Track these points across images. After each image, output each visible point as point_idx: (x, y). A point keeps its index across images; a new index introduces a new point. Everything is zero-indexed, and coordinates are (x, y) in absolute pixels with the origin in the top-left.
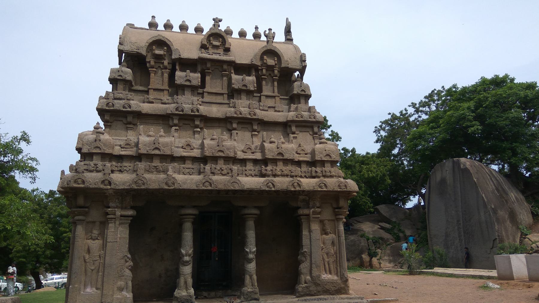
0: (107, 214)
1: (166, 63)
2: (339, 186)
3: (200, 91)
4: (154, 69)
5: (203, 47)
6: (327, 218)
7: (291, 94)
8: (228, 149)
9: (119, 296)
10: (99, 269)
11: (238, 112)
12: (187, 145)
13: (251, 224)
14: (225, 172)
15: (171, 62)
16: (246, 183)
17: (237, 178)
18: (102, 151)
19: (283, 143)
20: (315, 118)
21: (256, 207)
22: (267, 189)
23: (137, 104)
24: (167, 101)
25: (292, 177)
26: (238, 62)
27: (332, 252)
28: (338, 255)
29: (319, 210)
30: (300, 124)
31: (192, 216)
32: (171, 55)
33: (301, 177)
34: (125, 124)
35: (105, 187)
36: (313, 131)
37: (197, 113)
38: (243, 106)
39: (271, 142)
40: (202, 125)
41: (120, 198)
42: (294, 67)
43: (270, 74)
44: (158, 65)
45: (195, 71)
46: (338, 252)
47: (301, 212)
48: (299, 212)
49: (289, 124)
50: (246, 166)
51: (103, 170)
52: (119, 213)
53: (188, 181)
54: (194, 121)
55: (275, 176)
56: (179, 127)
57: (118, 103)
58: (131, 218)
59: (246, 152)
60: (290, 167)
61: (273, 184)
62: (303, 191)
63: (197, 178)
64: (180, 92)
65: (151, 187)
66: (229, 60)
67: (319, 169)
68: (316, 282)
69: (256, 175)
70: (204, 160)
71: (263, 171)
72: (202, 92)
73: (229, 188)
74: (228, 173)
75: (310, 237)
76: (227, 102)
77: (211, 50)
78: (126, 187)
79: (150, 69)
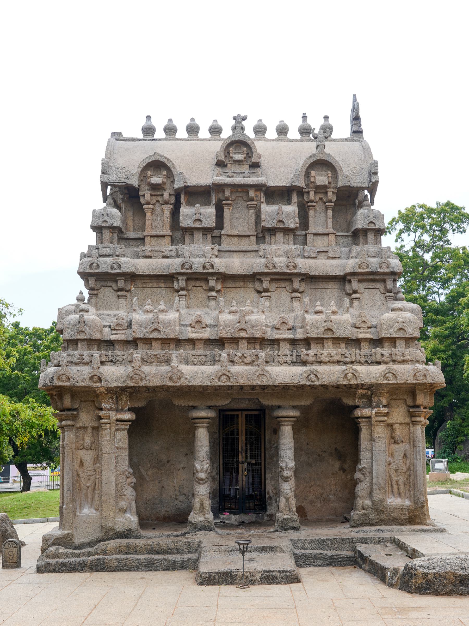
0: (100, 418)
1: (166, 196)
3: (217, 233)
4: (151, 206)
5: (220, 164)
7: (353, 229)
8: (253, 326)
9: (121, 520)
10: (95, 486)
11: (270, 265)
12: (197, 322)
13: (287, 431)
14: (248, 360)
15: (173, 193)
16: (277, 376)
17: (267, 368)
18: (87, 337)
19: (334, 313)
20: (388, 267)
21: (294, 407)
22: (308, 383)
23: (130, 263)
24: (170, 254)
25: (346, 363)
26: (271, 184)
27: (405, 469)
28: (412, 472)
29: (386, 410)
30: (365, 277)
32: (173, 182)
33: (360, 362)
34: (115, 290)
35: (95, 385)
36: (385, 287)
37: (211, 271)
38: (279, 254)
39: (316, 313)
40: (219, 287)
41: (115, 397)
42: (359, 185)
43: (321, 199)
45: (207, 203)
46: (412, 468)
47: (358, 413)
48: (355, 413)
49: (348, 278)
50: (279, 350)
51: (91, 362)
52: (114, 416)
53: (199, 375)
54: (207, 281)
55: (320, 363)
56: (188, 290)
57: (105, 263)
58: (130, 423)
59: (279, 329)
61: (316, 376)
62: (362, 385)
64: (187, 238)
65: (151, 384)
66: (256, 183)
67: (386, 350)
68: (378, 508)
69: (293, 363)
70: (220, 342)
71: (302, 356)
72: (218, 235)
73: (254, 384)
74: (253, 361)
75: (372, 449)
76: (255, 247)
78: (120, 385)
79: (144, 207)
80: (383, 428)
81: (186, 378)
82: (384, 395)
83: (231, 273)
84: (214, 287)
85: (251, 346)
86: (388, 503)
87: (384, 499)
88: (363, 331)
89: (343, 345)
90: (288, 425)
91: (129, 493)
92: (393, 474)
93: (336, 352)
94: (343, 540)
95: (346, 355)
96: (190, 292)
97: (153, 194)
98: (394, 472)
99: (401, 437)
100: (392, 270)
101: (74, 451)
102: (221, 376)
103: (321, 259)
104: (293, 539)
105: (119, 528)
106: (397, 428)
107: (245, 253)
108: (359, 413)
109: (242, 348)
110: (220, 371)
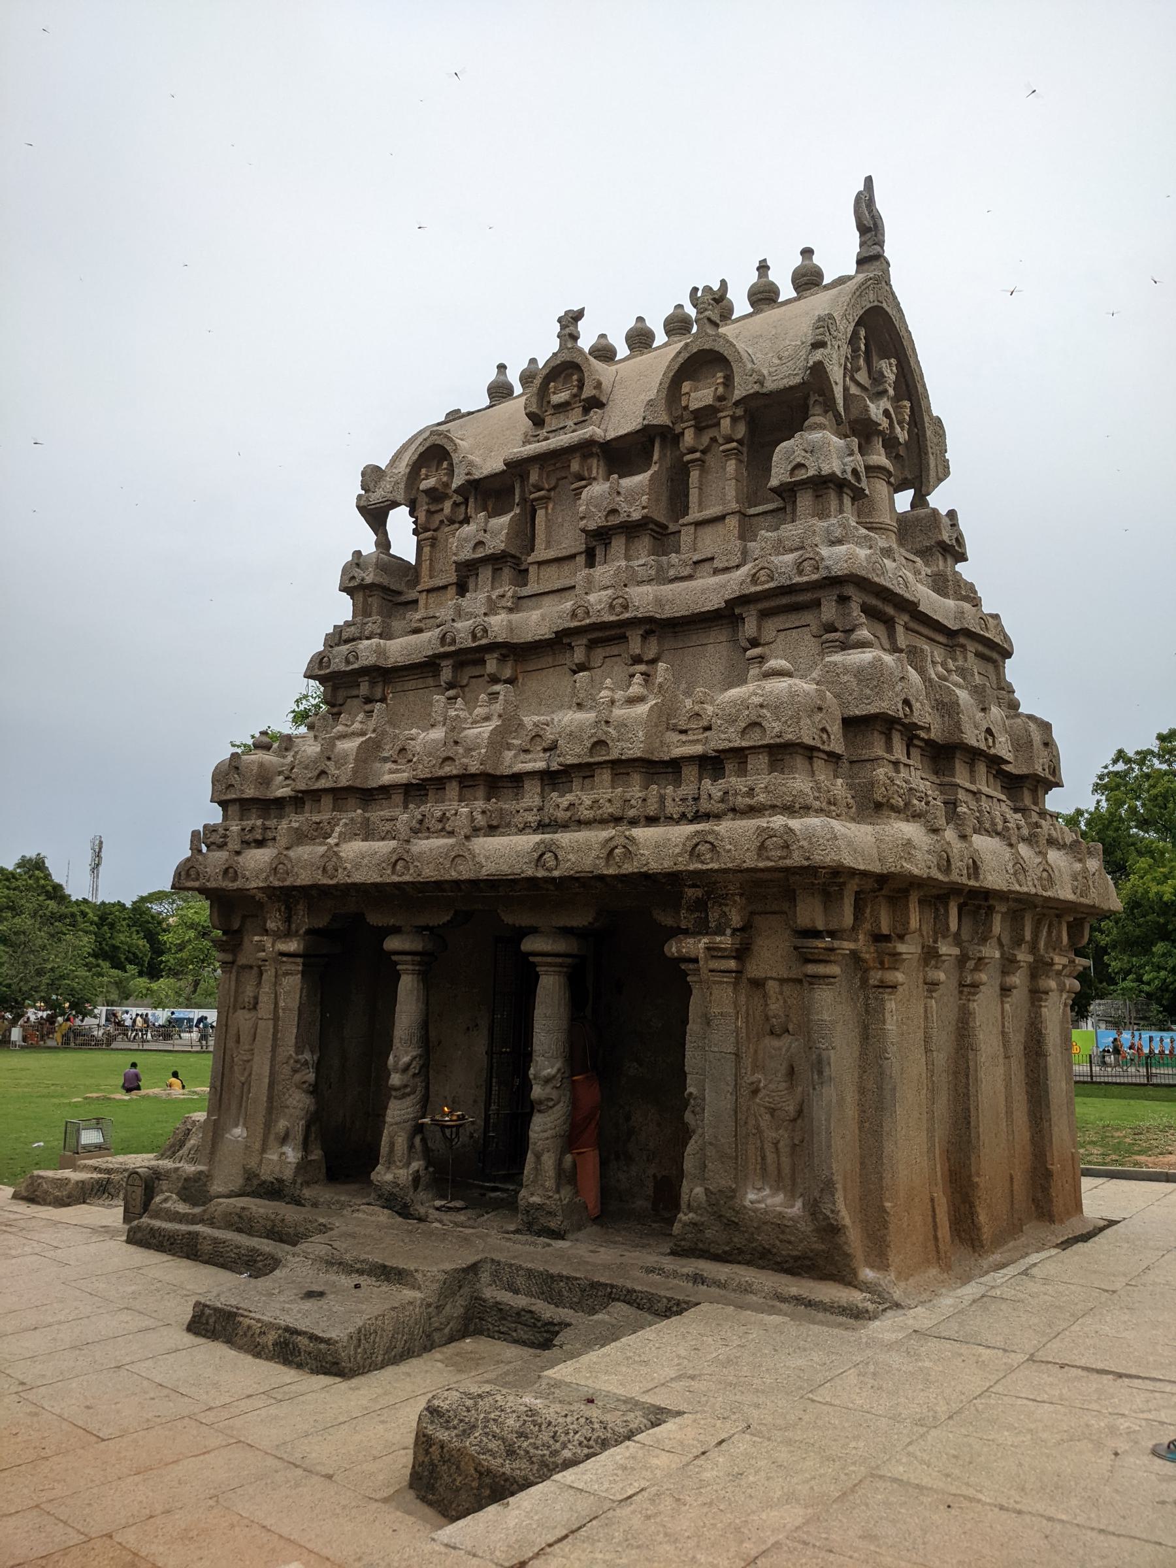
2: (762, 847)
4: (428, 534)
6: (774, 975)
8: (469, 750)
16: (487, 858)
22: (541, 873)
27: (791, 1108)
31: (409, 958)
37: (484, 641)
40: (507, 673)
44: (438, 518)
48: (666, 949)
49: (737, 611)
63: (384, 847)
65: (298, 883)
68: (724, 1209)
73: (447, 877)
77: (552, 422)
78: (261, 885)
80: (730, 990)
81: (345, 869)
82: (735, 902)
83: (522, 641)
84: (494, 675)
85: (467, 793)
86: (747, 1203)
88: (691, 738)
89: (636, 778)
90: (547, 973)
94: (594, 1285)
95: (633, 802)
96: (466, 689)
98: (767, 1117)
99: (783, 1019)
100: (823, 573)
101: (231, 1010)
102: (397, 861)
104: (497, 1259)
105: (266, 1174)
108: (674, 949)
109: (450, 800)
110: (394, 850)
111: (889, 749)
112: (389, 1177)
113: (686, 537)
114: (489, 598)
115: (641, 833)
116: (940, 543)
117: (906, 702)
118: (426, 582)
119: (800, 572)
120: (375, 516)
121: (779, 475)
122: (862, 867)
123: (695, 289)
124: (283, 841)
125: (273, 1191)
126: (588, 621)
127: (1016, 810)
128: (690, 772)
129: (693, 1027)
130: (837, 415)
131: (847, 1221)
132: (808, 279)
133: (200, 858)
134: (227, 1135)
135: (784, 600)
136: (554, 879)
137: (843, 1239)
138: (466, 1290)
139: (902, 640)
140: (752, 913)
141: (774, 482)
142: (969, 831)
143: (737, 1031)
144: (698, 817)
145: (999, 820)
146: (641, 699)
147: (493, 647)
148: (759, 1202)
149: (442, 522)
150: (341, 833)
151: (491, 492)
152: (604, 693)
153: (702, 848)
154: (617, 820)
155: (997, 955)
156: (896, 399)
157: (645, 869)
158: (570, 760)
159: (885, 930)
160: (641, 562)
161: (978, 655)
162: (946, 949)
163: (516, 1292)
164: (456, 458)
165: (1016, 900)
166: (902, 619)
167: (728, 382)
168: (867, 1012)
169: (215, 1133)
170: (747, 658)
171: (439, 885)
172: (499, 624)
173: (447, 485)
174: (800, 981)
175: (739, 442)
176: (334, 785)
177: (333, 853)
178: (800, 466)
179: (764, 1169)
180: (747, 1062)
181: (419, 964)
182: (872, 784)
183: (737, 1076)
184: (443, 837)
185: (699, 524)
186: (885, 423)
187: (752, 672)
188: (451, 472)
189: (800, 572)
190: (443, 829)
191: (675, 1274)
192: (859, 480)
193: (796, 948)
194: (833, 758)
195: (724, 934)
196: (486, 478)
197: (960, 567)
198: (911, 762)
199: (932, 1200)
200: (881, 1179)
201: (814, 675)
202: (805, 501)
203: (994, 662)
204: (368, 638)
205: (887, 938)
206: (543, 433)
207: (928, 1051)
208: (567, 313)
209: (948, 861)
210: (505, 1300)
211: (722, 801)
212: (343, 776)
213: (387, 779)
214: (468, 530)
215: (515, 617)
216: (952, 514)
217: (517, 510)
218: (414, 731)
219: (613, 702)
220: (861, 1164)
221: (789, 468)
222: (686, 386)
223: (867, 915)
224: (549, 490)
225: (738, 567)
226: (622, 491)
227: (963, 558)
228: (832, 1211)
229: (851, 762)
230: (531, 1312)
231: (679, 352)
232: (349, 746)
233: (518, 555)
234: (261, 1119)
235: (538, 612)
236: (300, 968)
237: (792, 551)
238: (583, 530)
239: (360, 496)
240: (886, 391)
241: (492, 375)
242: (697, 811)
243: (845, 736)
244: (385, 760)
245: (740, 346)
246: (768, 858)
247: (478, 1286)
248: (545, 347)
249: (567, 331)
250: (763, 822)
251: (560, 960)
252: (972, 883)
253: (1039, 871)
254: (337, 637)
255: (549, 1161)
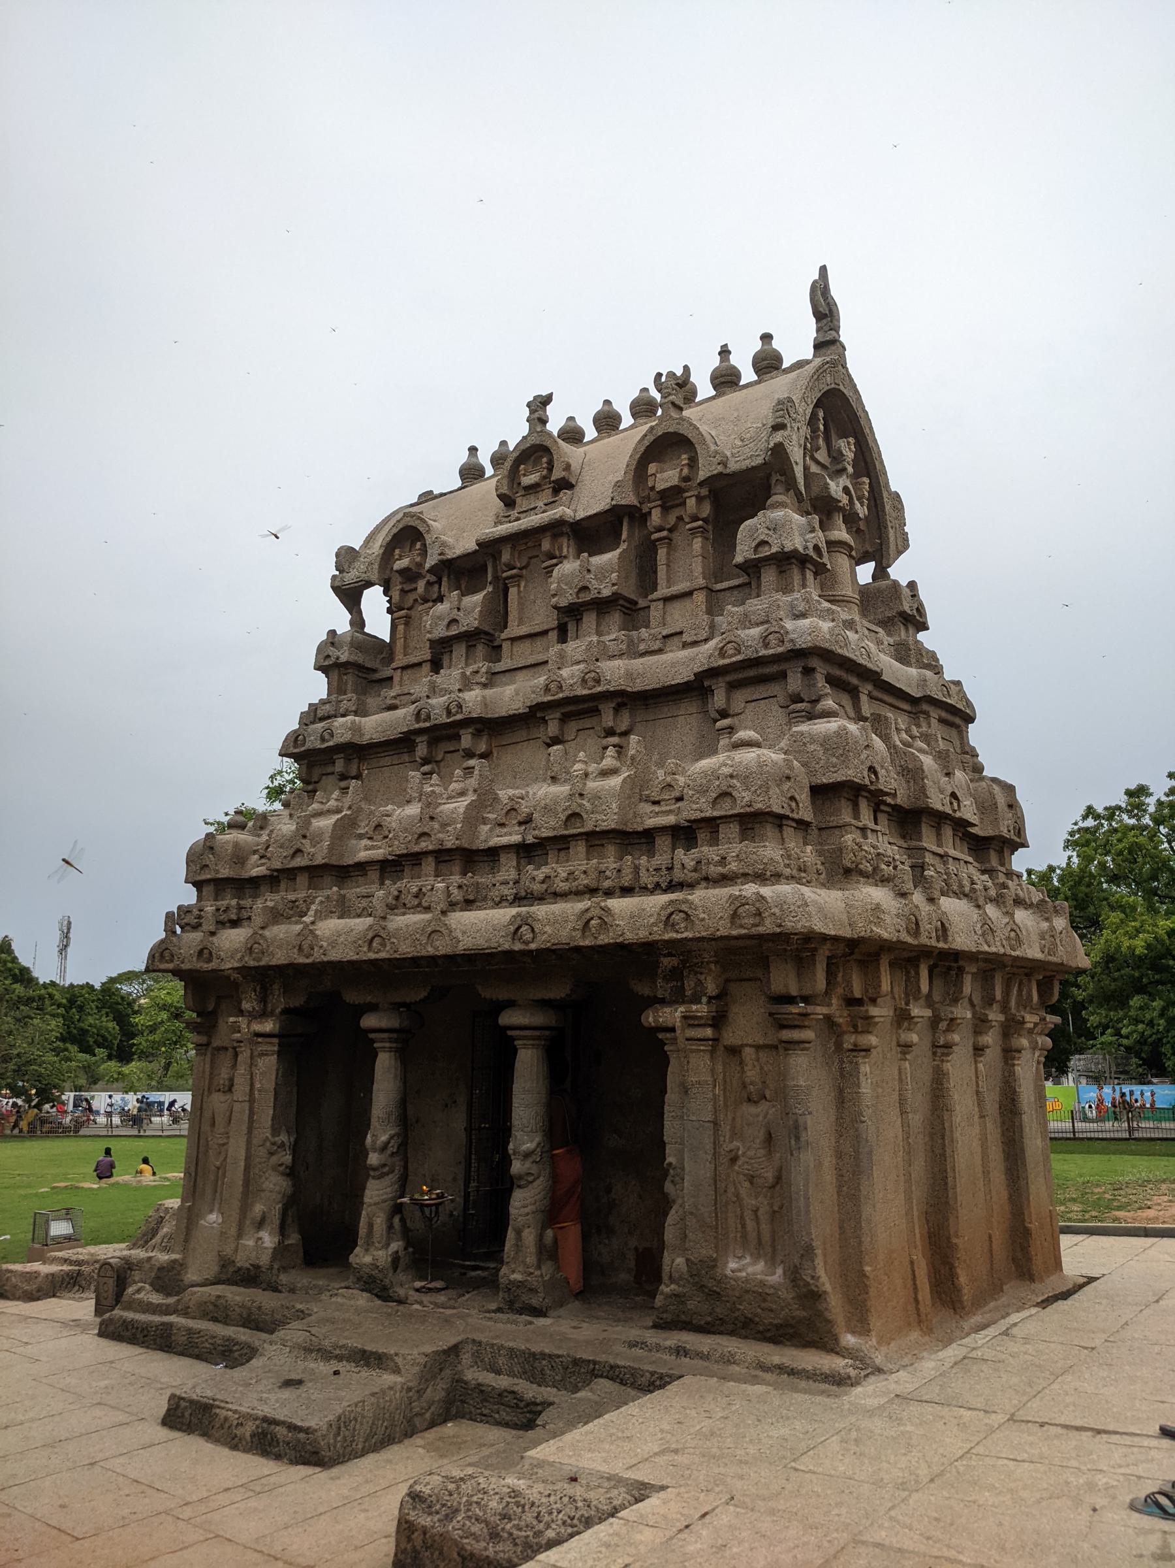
2: (735, 915)
6: (750, 1042)
8: (444, 825)
16: (464, 933)
22: (518, 946)
27: (770, 1175)
31: (385, 1035)
37: (459, 717)
40: (482, 747)
41: (258, 989)
43: (680, 518)
44: (411, 597)
49: (706, 684)
60: (609, 861)
63: (360, 924)
68: (704, 1278)
73: (424, 953)
77: (523, 503)
78: (236, 965)
80: (707, 1057)
81: (321, 947)
82: (710, 970)
84: (469, 749)
85: (442, 866)
86: (728, 1272)
87: (715, 1260)
88: (664, 808)
89: (611, 850)
90: (525, 1046)
91: (271, 1186)
92: (745, 1188)
93: (583, 868)
94: (576, 1362)
95: (608, 873)
96: (442, 764)
97: (407, 587)
98: (747, 1184)
99: (760, 1086)
100: (789, 646)
102: (373, 938)
103: (671, 651)
105: (242, 1261)
106: (748, 1059)
107: (536, 670)
108: (651, 1019)
110: (371, 927)
111: (857, 816)
112: (368, 1259)
113: (655, 612)
114: (463, 674)
115: (617, 904)
116: (902, 614)
117: (872, 769)
118: (400, 660)
119: (766, 645)
120: (350, 595)
121: (743, 552)
122: (833, 933)
123: (659, 375)
124: (258, 920)
125: (249, 1277)
126: (561, 695)
127: (983, 872)
128: (664, 843)
129: (671, 1097)
130: (798, 494)
131: (828, 1287)
132: (768, 363)
133: (174, 939)
134: (202, 1222)
135: (751, 673)
136: (531, 951)
137: (824, 1305)
138: (447, 1372)
139: (866, 709)
140: (728, 981)
141: (739, 559)
142: (936, 894)
143: (715, 1099)
144: (672, 887)
145: (966, 883)
146: (614, 772)
147: (468, 722)
148: (740, 1270)
149: (416, 600)
150: (316, 911)
151: (464, 571)
152: (577, 766)
153: (676, 917)
154: (592, 891)
155: (969, 1015)
156: (856, 476)
157: (621, 939)
158: (545, 833)
159: (857, 995)
160: (613, 637)
161: (942, 721)
162: (918, 1011)
163: (498, 1372)
164: (429, 539)
165: (986, 960)
166: (866, 688)
167: (693, 463)
168: (842, 1076)
169: (189, 1219)
170: (717, 729)
171: (415, 961)
172: (473, 700)
173: (420, 565)
174: (776, 1048)
175: (705, 520)
176: (310, 863)
177: (309, 931)
178: (764, 543)
179: (744, 1236)
180: (726, 1129)
181: (396, 1041)
182: (841, 850)
183: (716, 1144)
184: (419, 912)
185: (667, 600)
186: (845, 500)
187: (722, 743)
188: (424, 552)
189: (766, 645)
190: (419, 905)
191: (658, 1348)
192: (820, 555)
193: (771, 1014)
194: (802, 825)
195: (700, 1003)
196: (459, 557)
197: (921, 636)
198: (878, 828)
199: (912, 1263)
200: (860, 1243)
201: (782, 745)
202: (769, 576)
203: (957, 727)
204: (343, 716)
205: (859, 1002)
206: (514, 513)
207: (903, 1112)
208: (535, 398)
209: (917, 924)
210: (487, 1381)
211: (695, 870)
212: (319, 854)
213: (363, 856)
214: (441, 608)
215: (488, 692)
216: (912, 585)
217: (490, 589)
218: (390, 807)
219: (586, 775)
220: (840, 1228)
221: (754, 545)
222: (652, 468)
223: (839, 979)
224: (521, 569)
225: (706, 640)
226: (592, 569)
227: (923, 627)
228: (813, 1277)
229: (820, 829)
230: (513, 1392)
231: (645, 435)
232: (326, 823)
233: (492, 632)
234: (236, 1204)
235: (512, 687)
236: (276, 1049)
237: (758, 625)
238: (555, 607)
239: (334, 577)
240: (845, 469)
241: (464, 457)
242: (671, 881)
243: (813, 803)
244: (361, 837)
245: (703, 428)
246: (741, 926)
247: (459, 1368)
248: (516, 431)
249: (536, 415)
250: (735, 890)
251: (537, 1033)
252: (941, 945)
253: (1006, 932)
254: (313, 715)
255: (529, 1236)
